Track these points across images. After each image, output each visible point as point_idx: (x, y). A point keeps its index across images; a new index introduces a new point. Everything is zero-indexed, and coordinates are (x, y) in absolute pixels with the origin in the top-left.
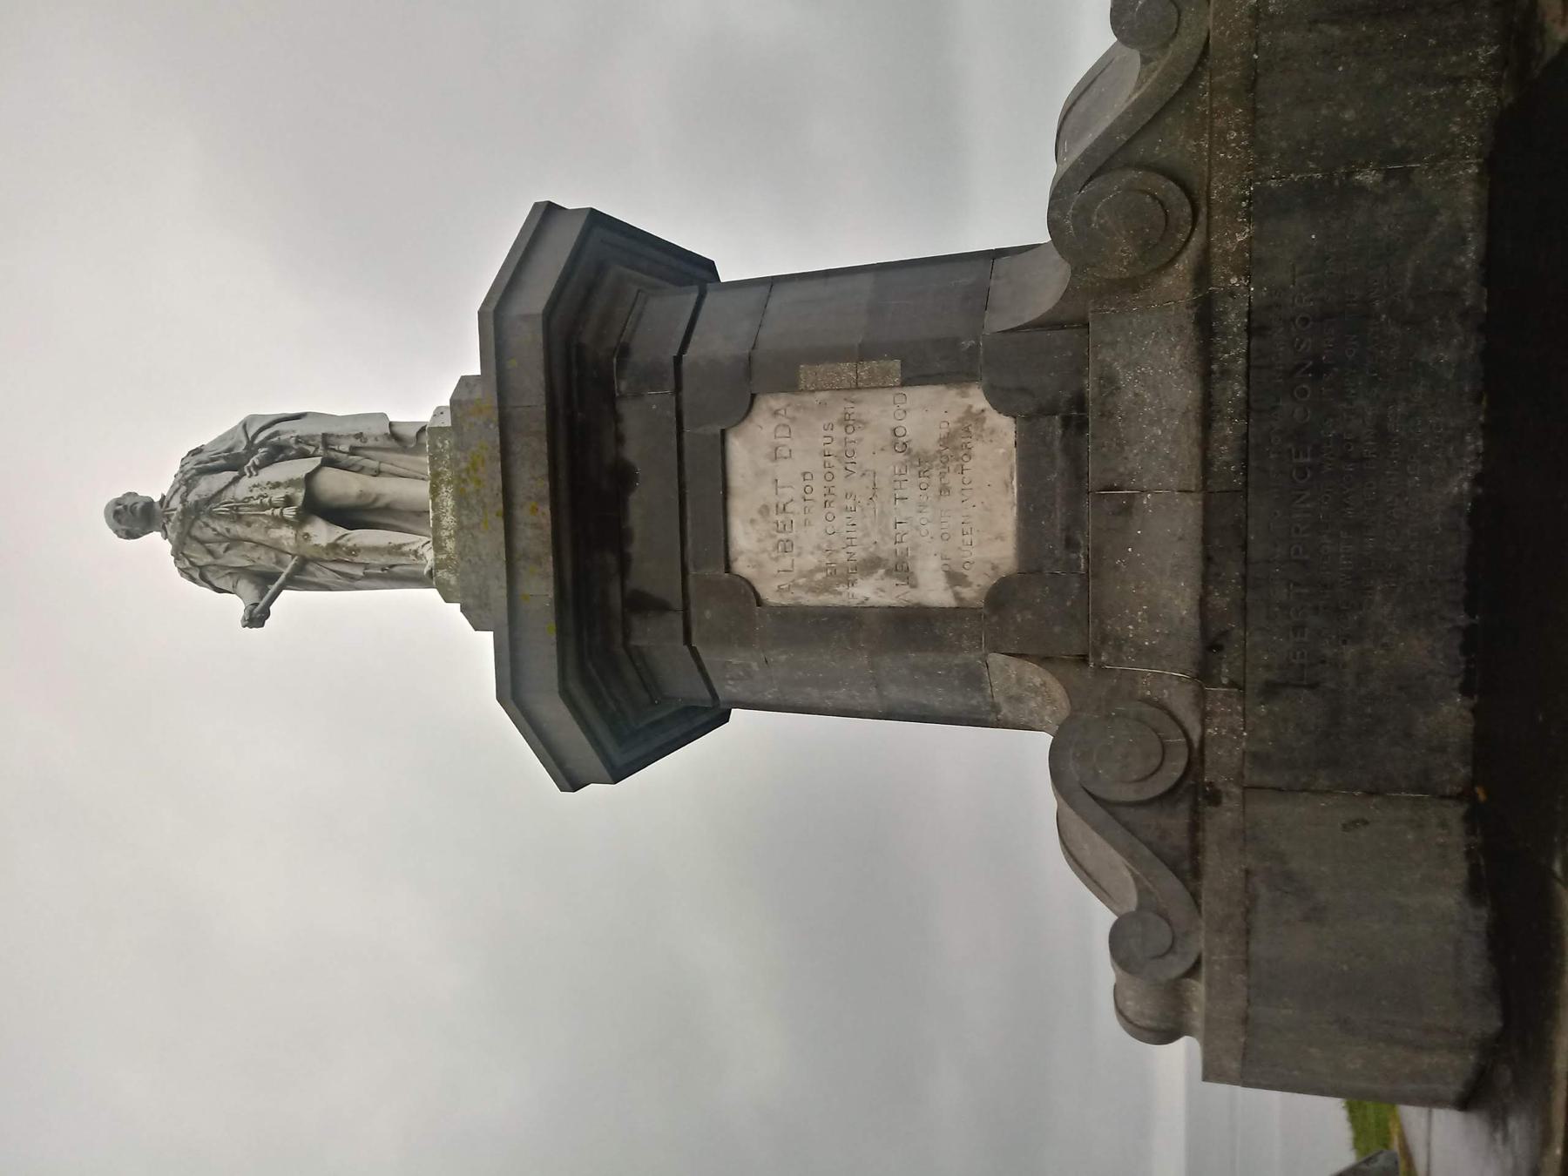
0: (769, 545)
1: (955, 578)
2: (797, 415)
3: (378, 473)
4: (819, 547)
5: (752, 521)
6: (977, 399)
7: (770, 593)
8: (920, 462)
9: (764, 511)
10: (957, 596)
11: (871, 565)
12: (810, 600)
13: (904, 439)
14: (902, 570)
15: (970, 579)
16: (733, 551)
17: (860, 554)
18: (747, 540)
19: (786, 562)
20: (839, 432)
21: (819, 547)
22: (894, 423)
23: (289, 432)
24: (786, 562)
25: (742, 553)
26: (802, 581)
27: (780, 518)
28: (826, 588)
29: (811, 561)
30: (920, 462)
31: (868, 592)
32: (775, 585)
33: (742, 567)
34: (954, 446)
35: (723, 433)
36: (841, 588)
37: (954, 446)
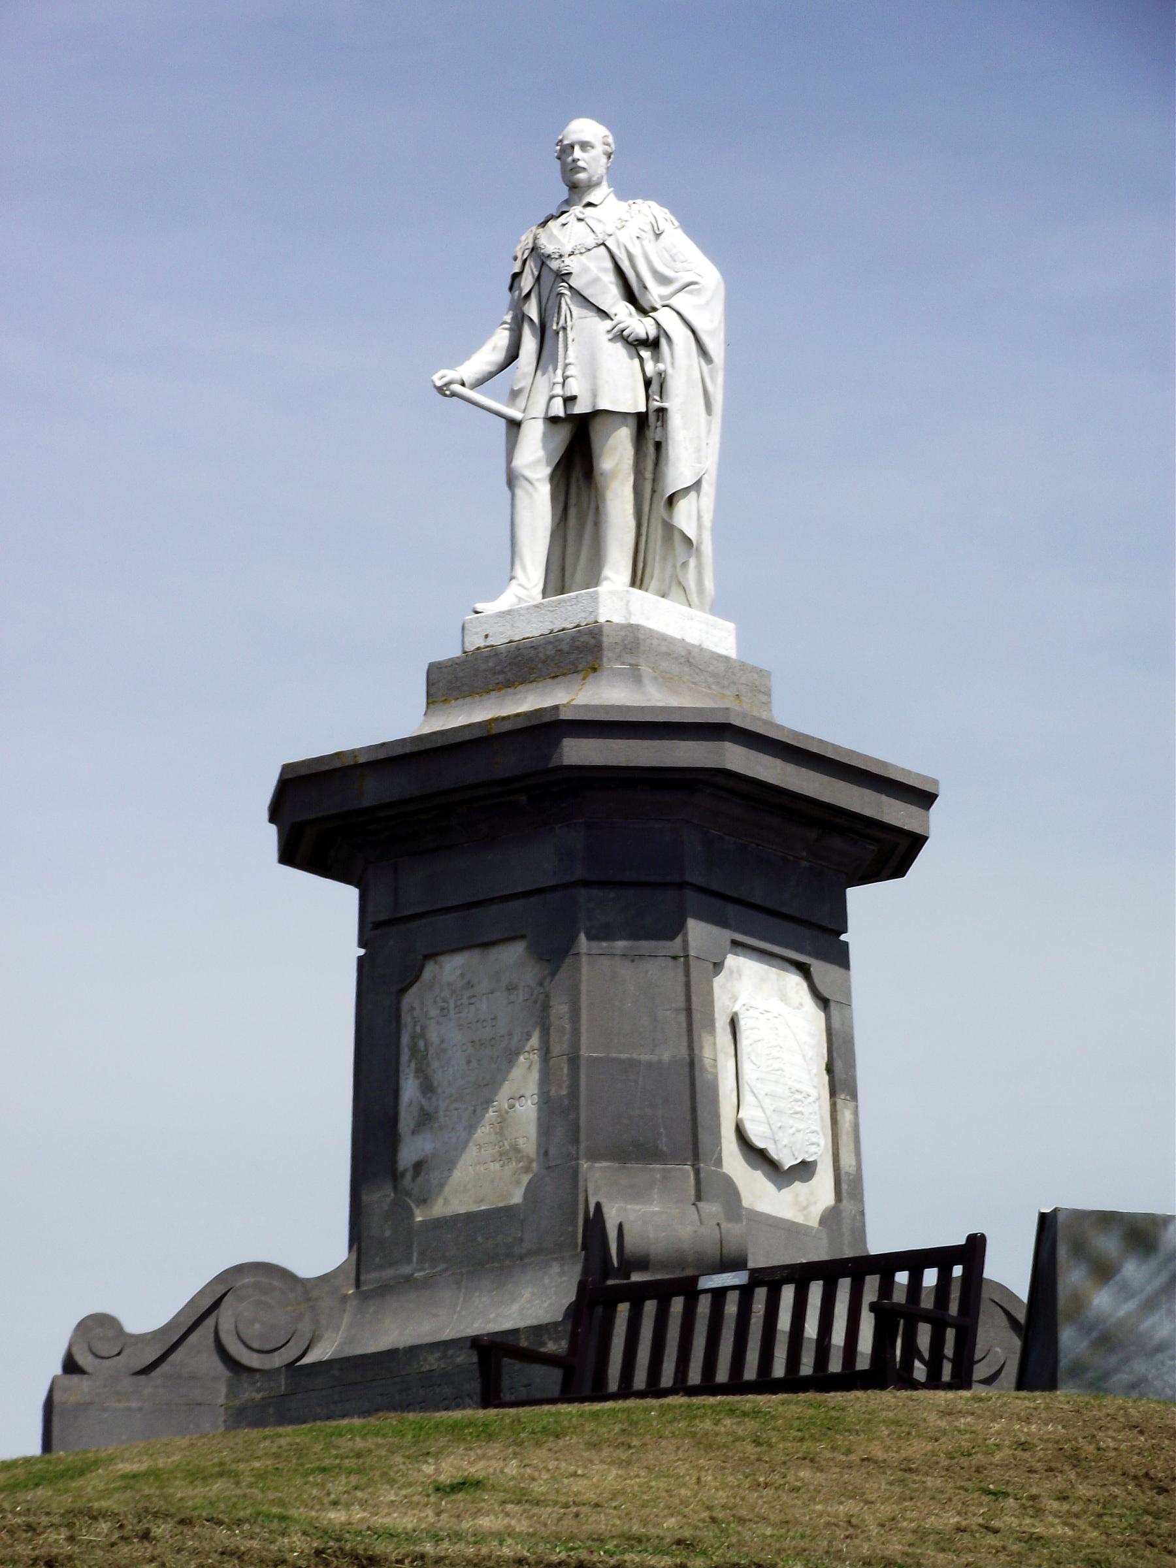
0: (446, 993)
1: (418, 1167)
2: (538, 1005)
4: (442, 1042)
5: (462, 975)
10: (406, 1170)
12: (405, 1039)
13: (517, 1105)
14: (425, 1119)
15: (420, 1179)
16: (442, 959)
17: (438, 1078)
19: (434, 1012)
21: (442, 1042)
22: (528, 1094)
24: (434, 1012)
25: (441, 967)
26: (418, 1029)
27: (465, 1001)
28: (414, 1051)
29: (433, 1035)
31: (409, 1090)
32: (417, 1005)
35: (523, 937)
36: (413, 1065)
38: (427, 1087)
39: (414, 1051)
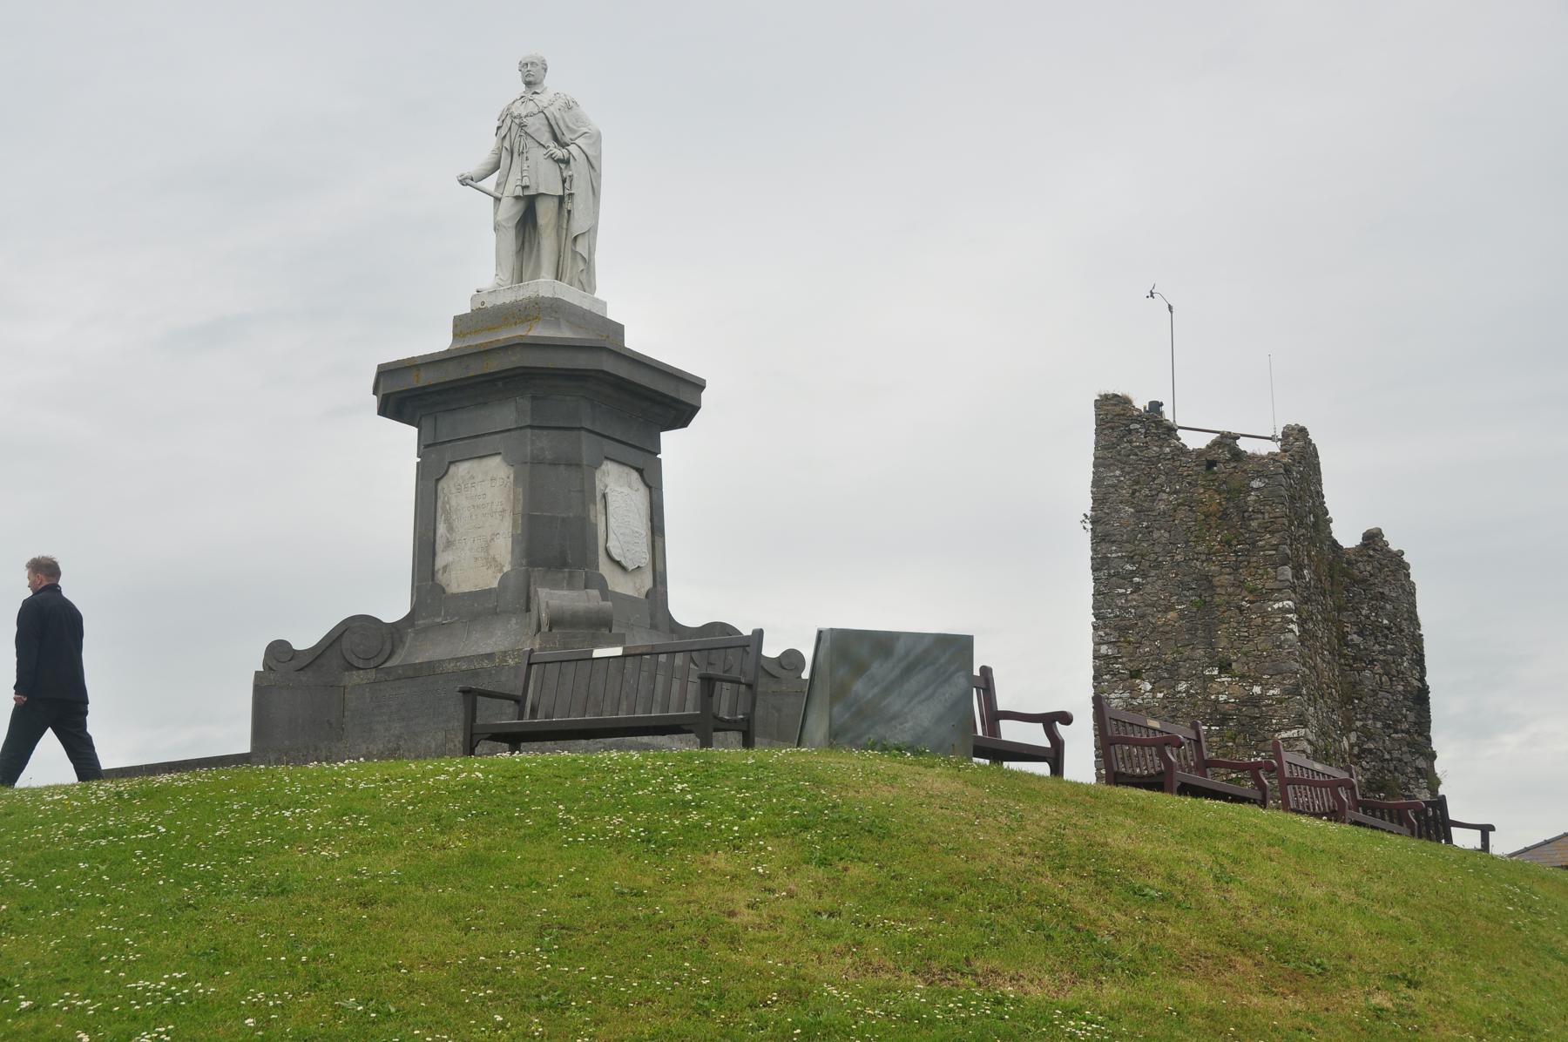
1: (445, 568)
3: (559, 228)
6: (506, 569)
7: (442, 484)
8: (487, 548)
9: (472, 477)
11: (450, 529)
14: (449, 544)
17: (456, 524)
18: (462, 470)
20: (500, 508)
23: (578, 169)
29: (453, 503)
30: (487, 548)
31: (442, 529)
33: (453, 469)
34: (491, 562)
37: (491, 562)
38: (450, 529)
39: (444, 509)
